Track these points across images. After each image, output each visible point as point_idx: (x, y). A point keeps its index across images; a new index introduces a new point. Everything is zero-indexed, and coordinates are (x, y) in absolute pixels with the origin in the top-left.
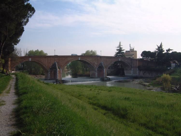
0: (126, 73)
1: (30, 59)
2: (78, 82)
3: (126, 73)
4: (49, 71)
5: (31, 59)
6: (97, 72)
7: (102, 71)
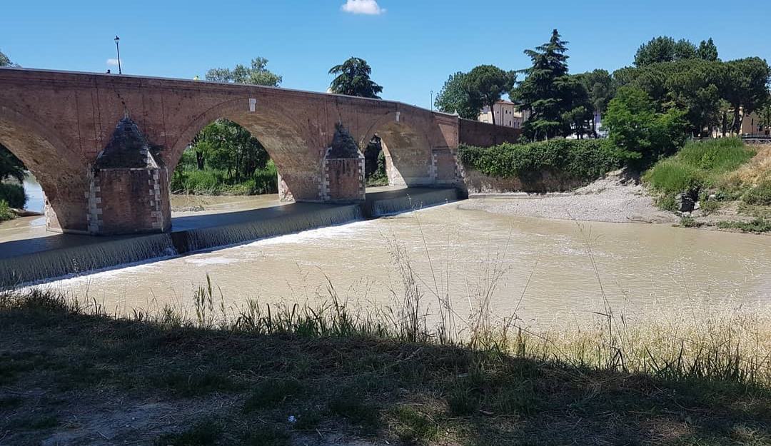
4: (91, 175)
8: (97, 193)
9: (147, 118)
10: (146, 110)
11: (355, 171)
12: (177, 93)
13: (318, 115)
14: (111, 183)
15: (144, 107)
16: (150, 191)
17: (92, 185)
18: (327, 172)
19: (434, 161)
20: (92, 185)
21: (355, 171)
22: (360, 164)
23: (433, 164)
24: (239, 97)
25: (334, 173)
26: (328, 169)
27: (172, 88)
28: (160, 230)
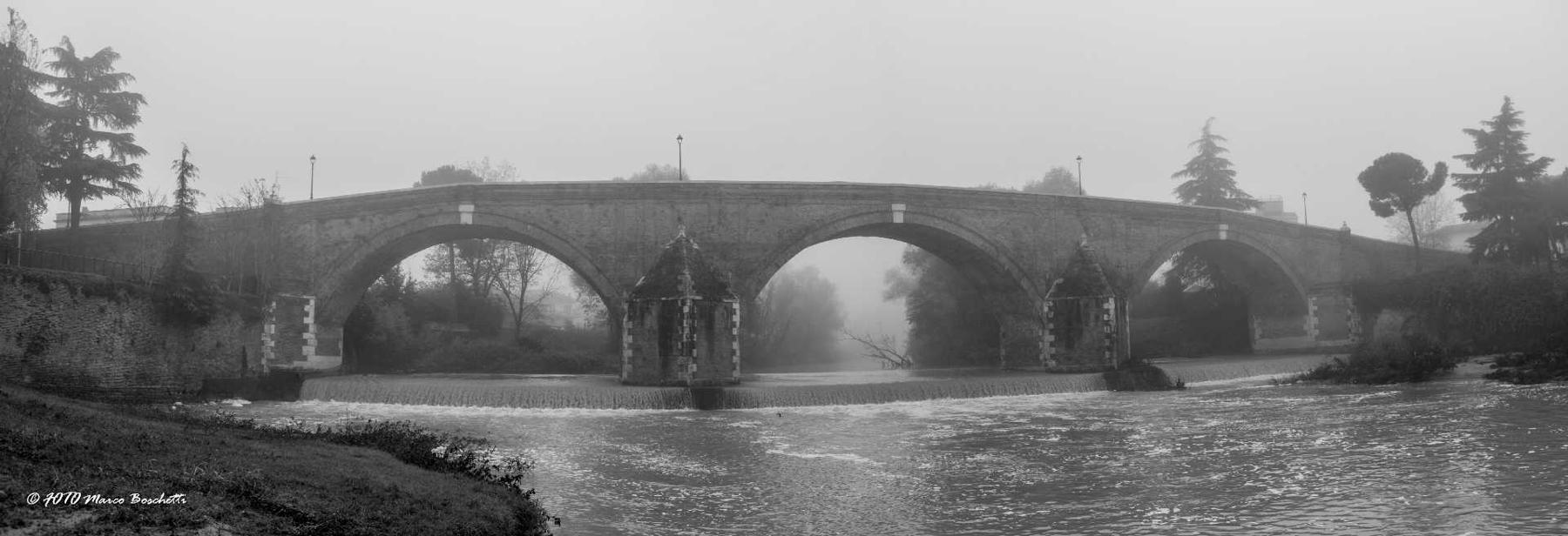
0: (1262, 337)
1: (462, 208)
2: (544, 404)
3: (1262, 337)
4: (626, 307)
5: (471, 208)
6: (1051, 326)
8: (629, 329)
10: (713, 224)
11: (1097, 318)
12: (763, 200)
14: (642, 316)
17: (625, 320)
18: (1050, 320)
19: (1312, 308)
20: (625, 320)
21: (1097, 318)
22: (1106, 306)
23: (1311, 313)
26: (1051, 315)
28: (686, 382)
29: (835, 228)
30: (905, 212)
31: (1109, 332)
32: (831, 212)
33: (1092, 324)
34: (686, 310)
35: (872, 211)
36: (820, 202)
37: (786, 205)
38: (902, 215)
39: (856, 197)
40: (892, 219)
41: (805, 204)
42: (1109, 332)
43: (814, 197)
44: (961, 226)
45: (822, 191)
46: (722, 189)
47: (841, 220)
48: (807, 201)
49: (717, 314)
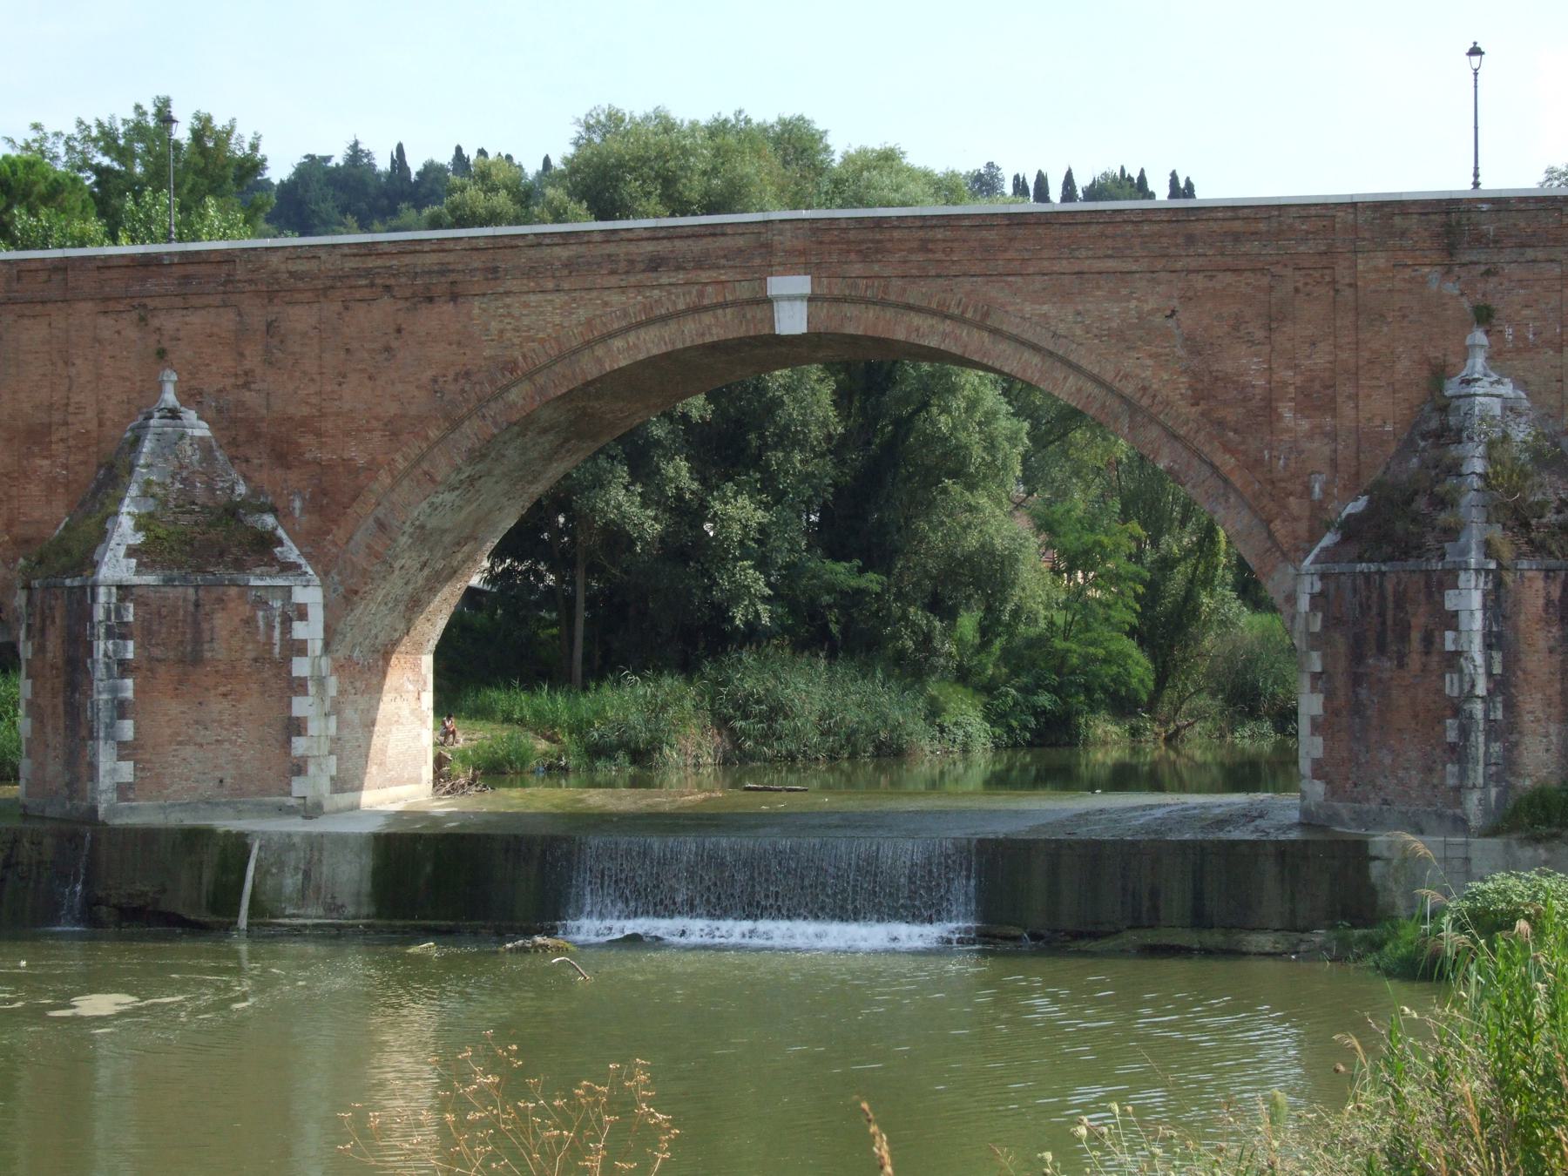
7: (1419, 619)
9: (247, 396)
10: (248, 365)
12: (388, 288)
13: (1273, 319)
15: (242, 355)
16: (89, 661)
18: (1316, 641)
21: (1429, 640)
22: (1451, 601)
24: (704, 276)
25: (1341, 643)
26: (1317, 626)
27: (368, 273)
29: (599, 361)
30: (811, 299)
31: (1455, 693)
32: (582, 314)
33: (1415, 661)
34: (99, 614)
35: (706, 302)
36: (550, 285)
37: (454, 297)
38: (801, 309)
39: (655, 264)
40: (773, 327)
41: (507, 293)
42: (1455, 693)
43: (532, 272)
44: (995, 332)
45: (557, 250)
46: (275, 260)
47: (612, 335)
48: (512, 284)
49: (222, 623)
